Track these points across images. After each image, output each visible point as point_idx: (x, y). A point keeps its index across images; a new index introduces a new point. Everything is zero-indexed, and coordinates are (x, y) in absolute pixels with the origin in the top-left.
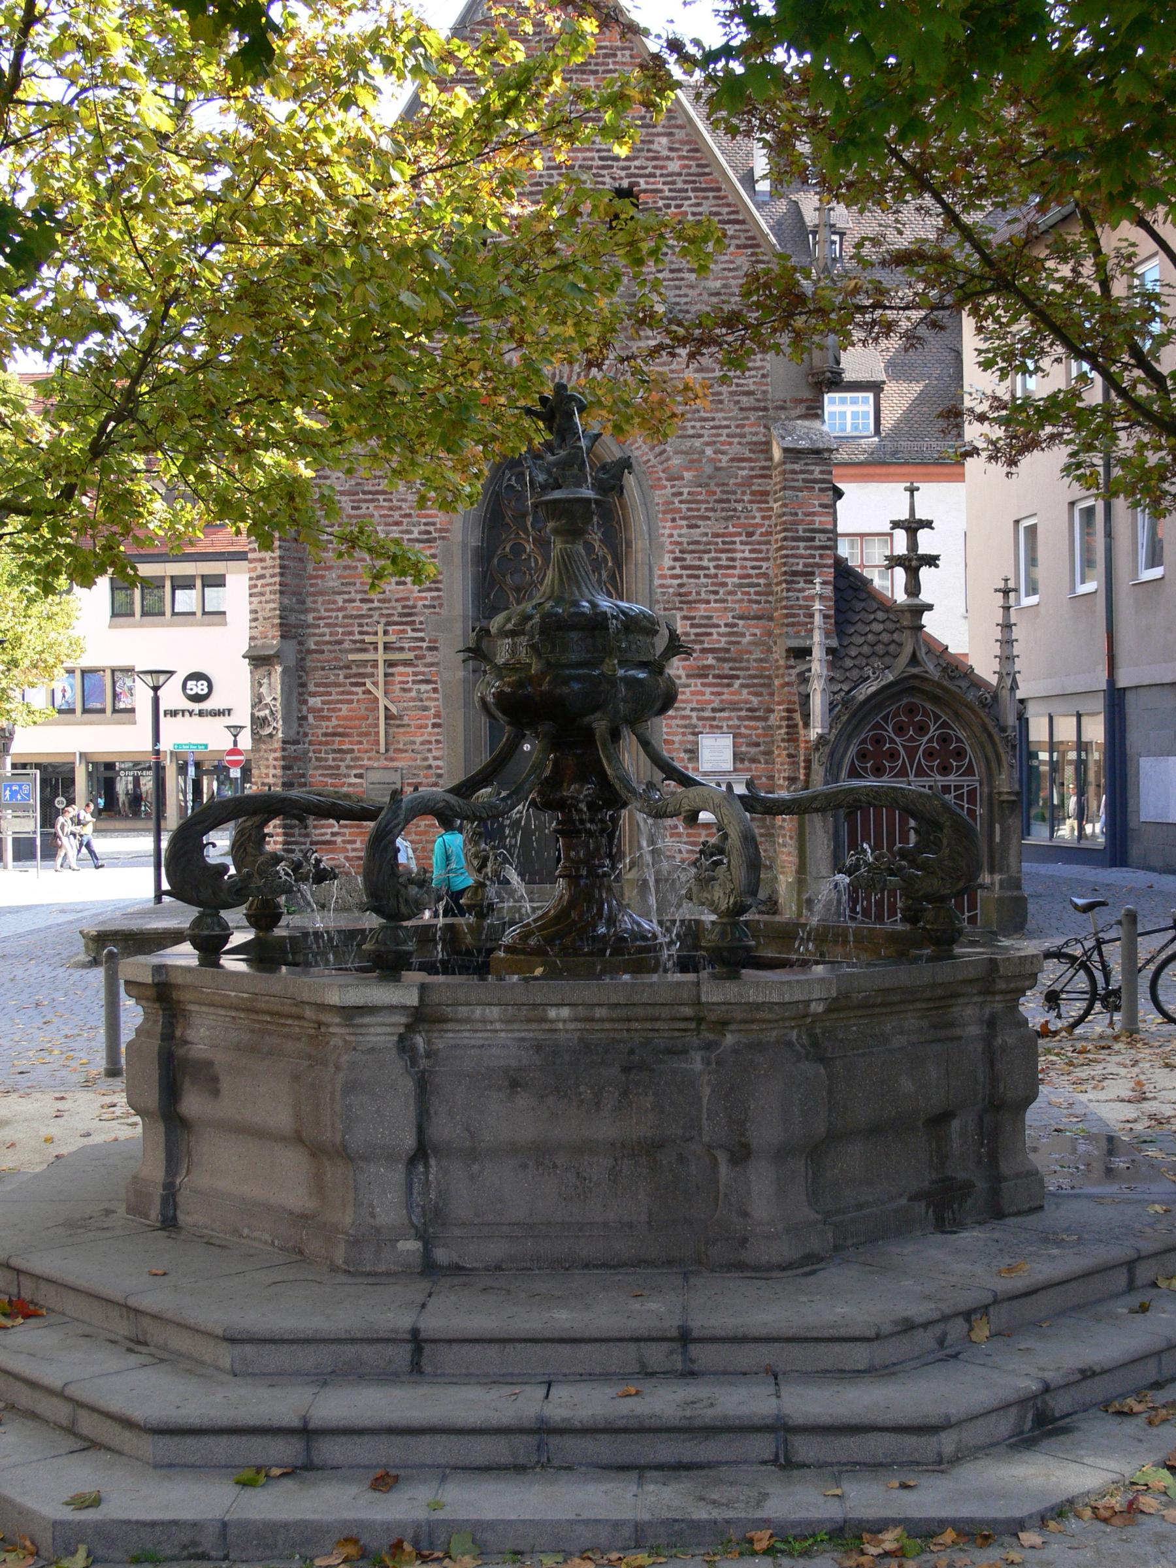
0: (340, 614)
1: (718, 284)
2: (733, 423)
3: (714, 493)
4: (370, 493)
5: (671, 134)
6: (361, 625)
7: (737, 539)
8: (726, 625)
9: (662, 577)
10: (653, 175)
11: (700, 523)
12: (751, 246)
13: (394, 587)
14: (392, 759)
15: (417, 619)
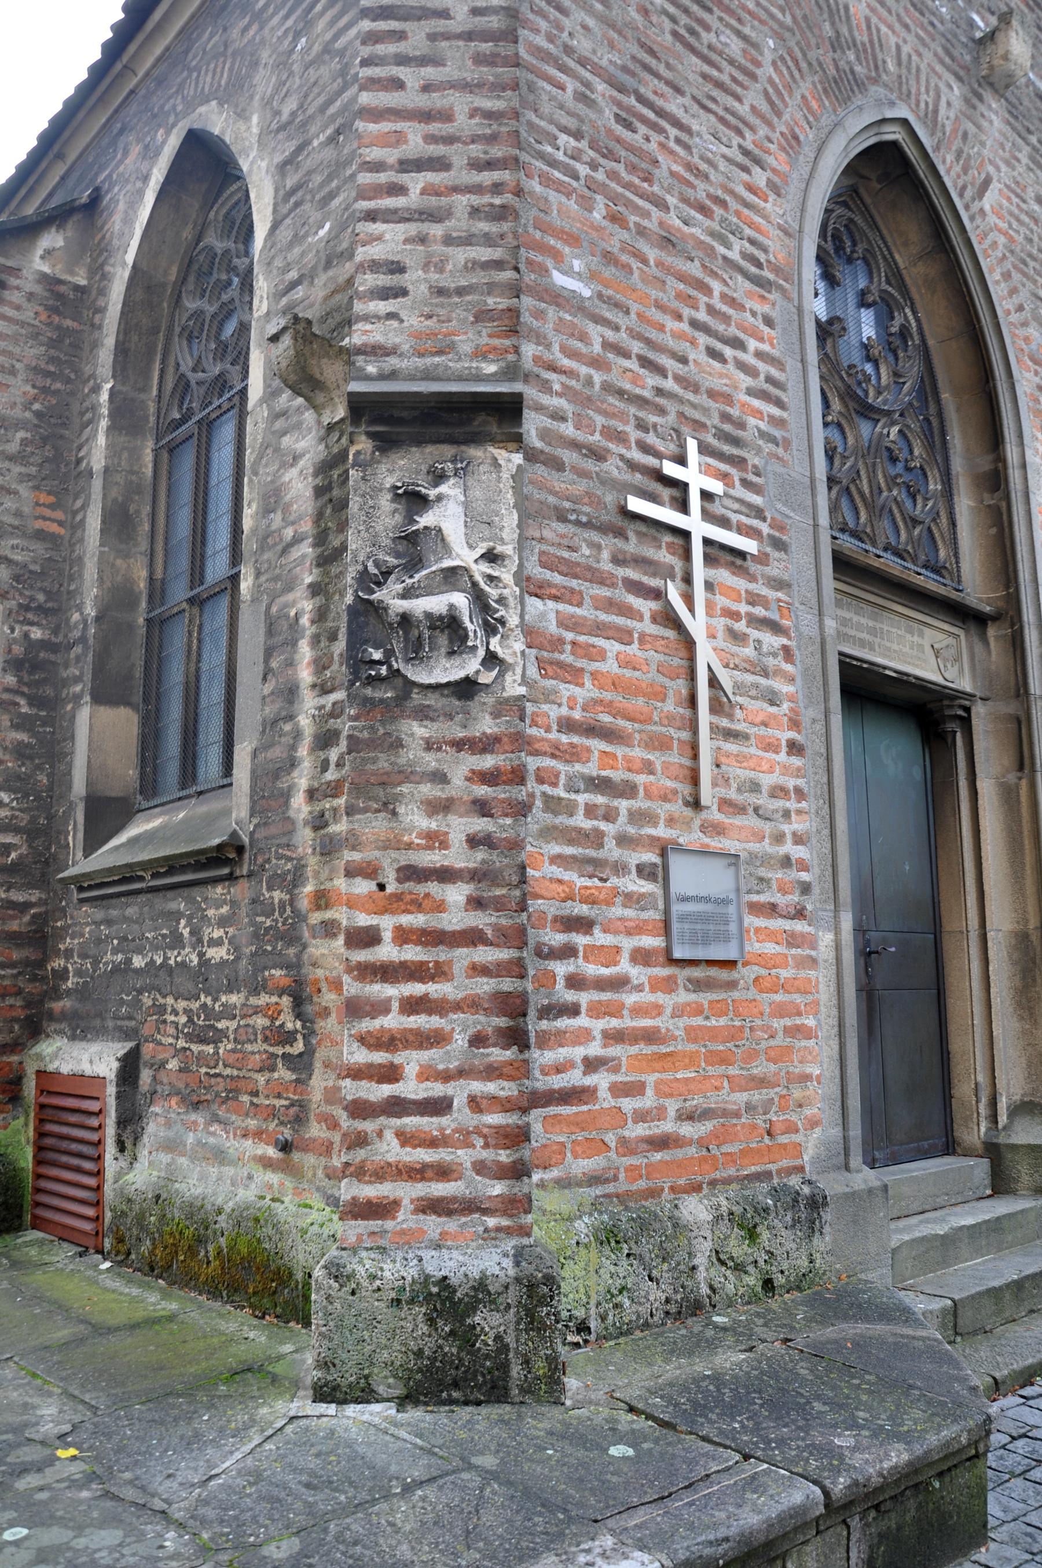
0: (598, 378)
6: (642, 426)
14: (717, 830)
15: (753, 460)
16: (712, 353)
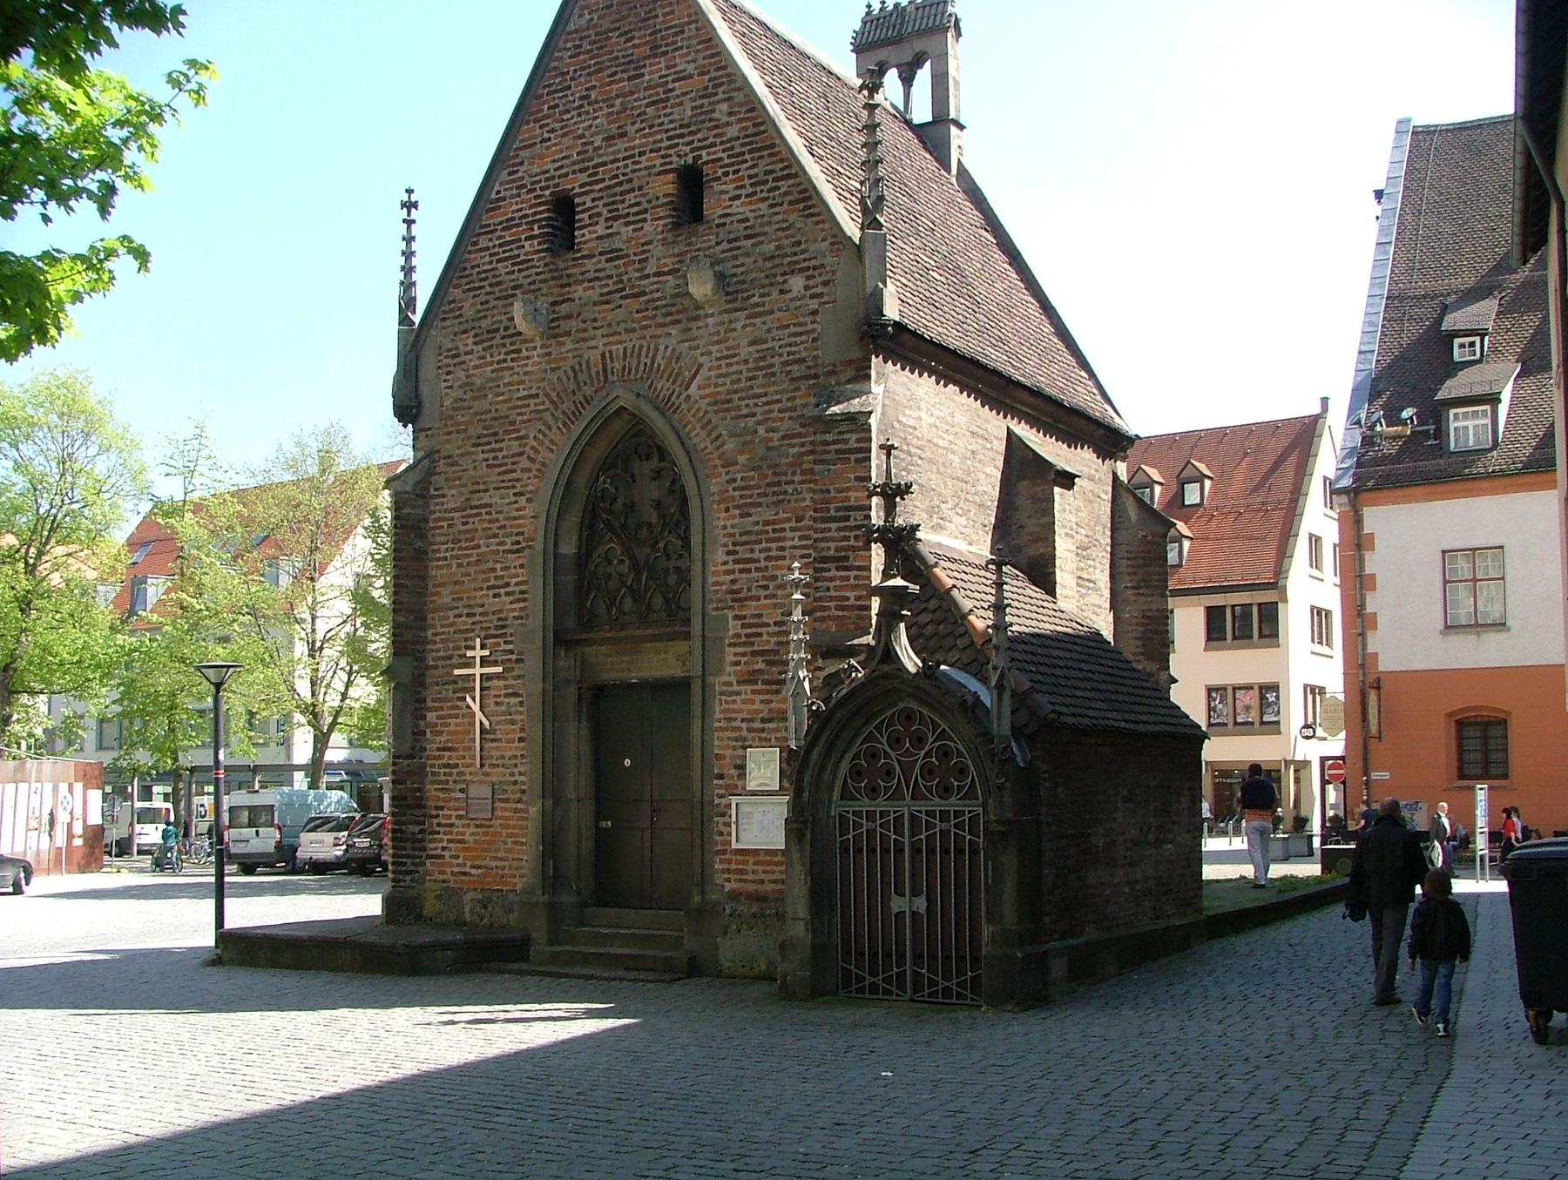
1: (772, 246)
2: (785, 397)
3: (766, 476)
4: (477, 507)
5: (730, 99)
7: (787, 526)
8: (776, 624)
9: (715, 573)
10: (714, 145)
11: (752, 511)
12: (803, 200)
13: (491, 600)
16: (495, 596)
